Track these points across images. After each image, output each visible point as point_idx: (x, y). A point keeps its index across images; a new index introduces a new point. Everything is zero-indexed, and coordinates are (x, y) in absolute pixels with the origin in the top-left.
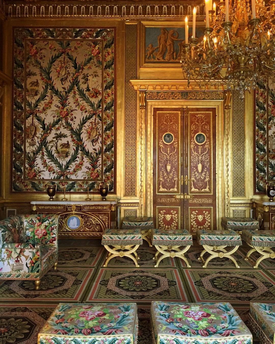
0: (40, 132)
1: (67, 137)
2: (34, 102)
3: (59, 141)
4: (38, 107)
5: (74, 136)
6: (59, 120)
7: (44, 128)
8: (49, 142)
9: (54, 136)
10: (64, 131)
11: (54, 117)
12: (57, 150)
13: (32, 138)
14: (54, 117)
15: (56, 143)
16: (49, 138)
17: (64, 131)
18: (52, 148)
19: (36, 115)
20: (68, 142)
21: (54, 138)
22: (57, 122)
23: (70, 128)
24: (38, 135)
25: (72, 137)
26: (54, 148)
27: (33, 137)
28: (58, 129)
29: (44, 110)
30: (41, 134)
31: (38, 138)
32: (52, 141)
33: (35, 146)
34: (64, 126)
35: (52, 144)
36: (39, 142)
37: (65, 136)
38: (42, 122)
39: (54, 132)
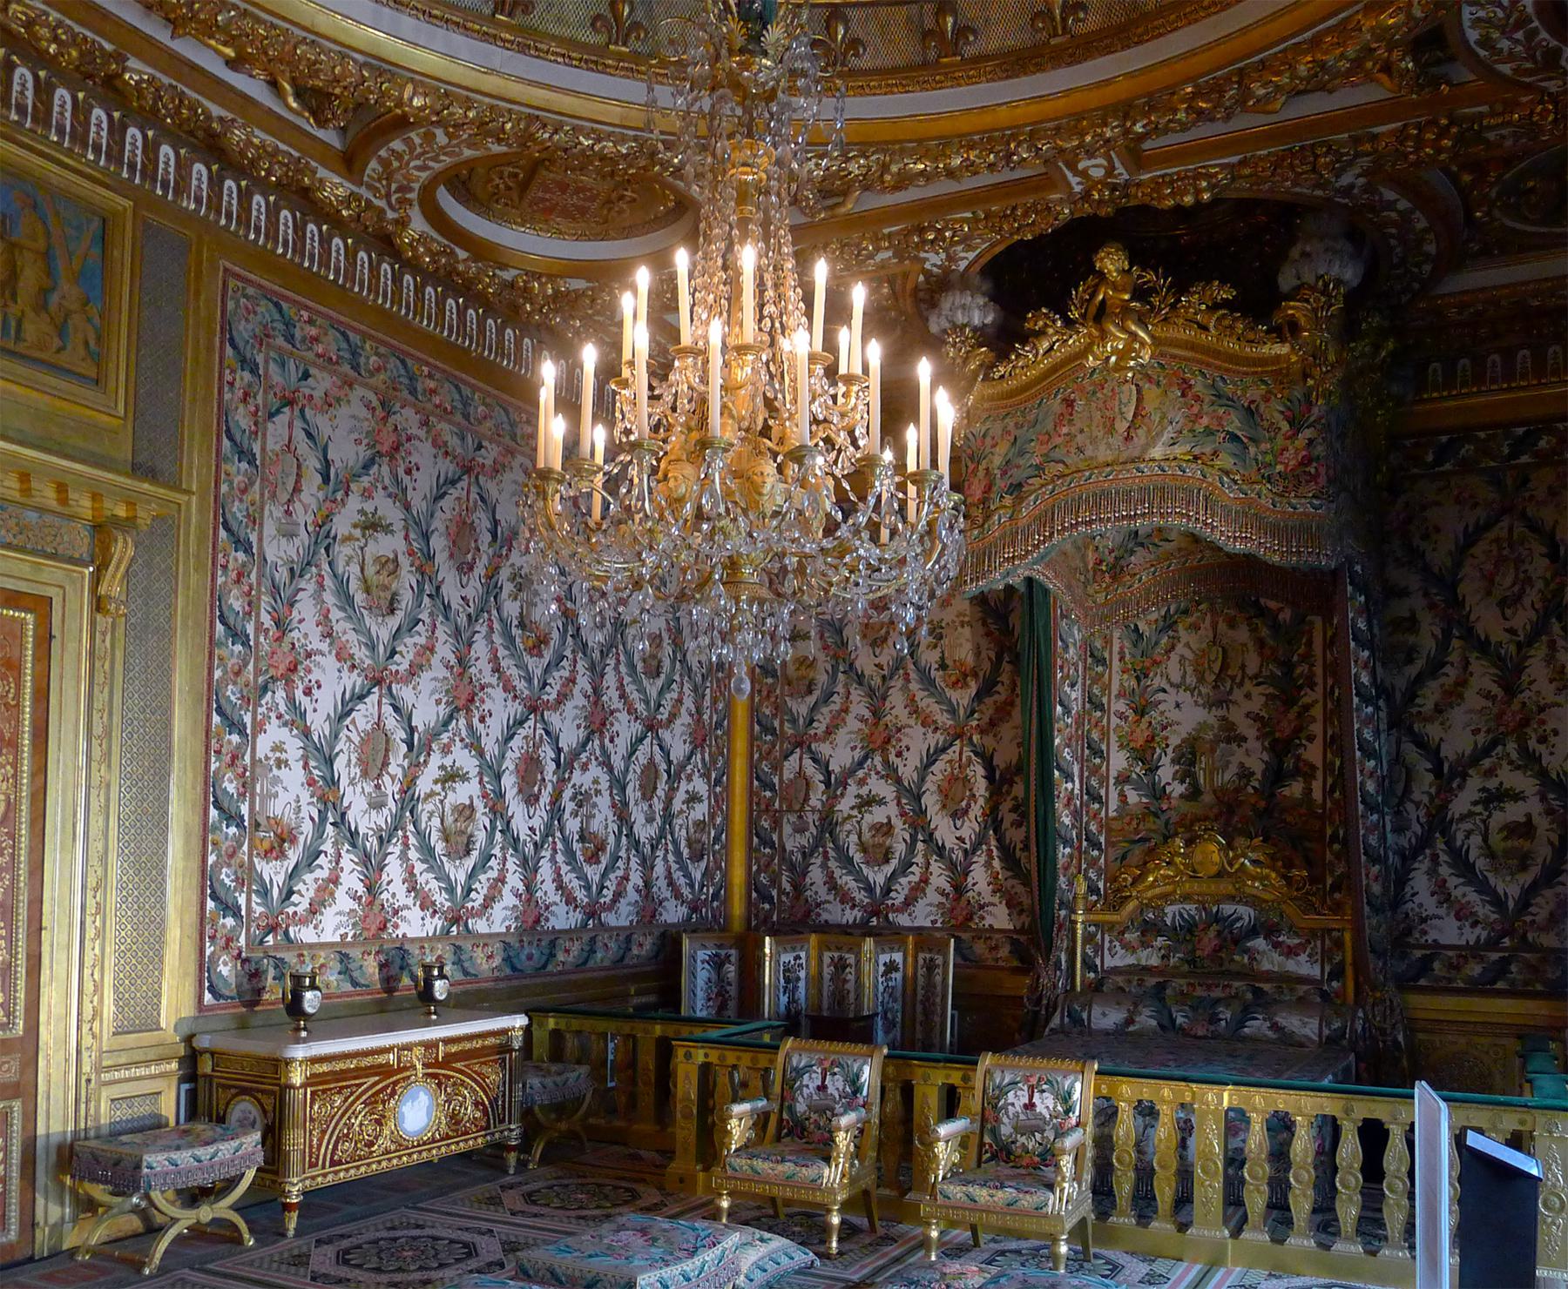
0: (1424, 784)
1: (1524, 799)
2: (1401, 683)
3: (1497, 815)
4: (1418, 701)
5: (1551, 796)
6: (1494, 743)
7: (1437, 771)
8: (1457, 816)
9: (1476, 796)
10: (1510, 778)
11: (1476, 732)
12: (1489, 847)
13: (1398, 805)
14: (1476, 732)
15: (1484, 821)
16: (1461, 803)
17: (1510, 778)
18: (1467, 837)
19: (1410, 730)
20: (1529, 816)
21: (1475, 803)
22: (1486, 751)
23: (1537, 768)
24: (1416, 796)
25: (1543, 799)
26: (1476, 840)
27: (1401, 803)
28: (1490, 773)
29: (1439, 710)
30: (1429, 794)
31: (1417, 805)
32: (1471, 814)
34: (1511, 763)
35: (1467, 826)
36: (1423, 820)
37: (1517, 797)
38: (1433, 753)
39: (1474, 784)
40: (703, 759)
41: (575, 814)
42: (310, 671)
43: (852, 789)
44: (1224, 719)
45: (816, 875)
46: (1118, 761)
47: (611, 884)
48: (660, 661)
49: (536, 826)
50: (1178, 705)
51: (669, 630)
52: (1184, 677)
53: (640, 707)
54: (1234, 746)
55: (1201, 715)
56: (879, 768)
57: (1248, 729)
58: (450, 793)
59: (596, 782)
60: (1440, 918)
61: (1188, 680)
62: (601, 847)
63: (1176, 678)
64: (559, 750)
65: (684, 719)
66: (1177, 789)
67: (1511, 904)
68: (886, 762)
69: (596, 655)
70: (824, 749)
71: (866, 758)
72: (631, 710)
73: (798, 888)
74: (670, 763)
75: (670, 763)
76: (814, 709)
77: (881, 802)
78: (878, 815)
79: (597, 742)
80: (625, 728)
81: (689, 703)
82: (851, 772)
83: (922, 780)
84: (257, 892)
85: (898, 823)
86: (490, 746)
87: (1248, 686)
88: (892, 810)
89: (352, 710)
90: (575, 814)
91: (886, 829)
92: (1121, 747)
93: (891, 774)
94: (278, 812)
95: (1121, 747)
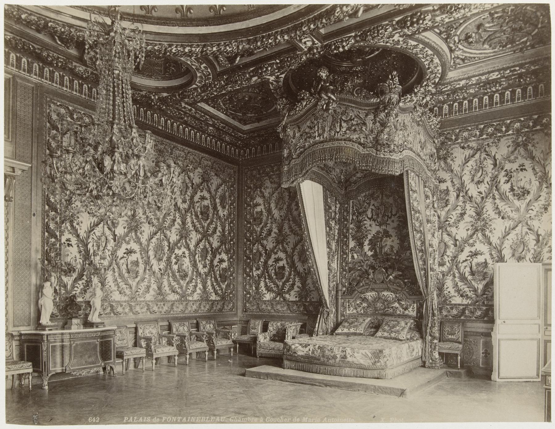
0: (451, 251)
3: (475, 259)
7: (455, 245)
8: (461, 261)
13: (442, 256)
15: (471, 262)
16: (462, 257)
20: (486, 260)
24: (448, 253)
28: (472, 245)
31: (448, 256)
32: (466, 260)
33: (446, 266)
40: (225, 247)
41: (176, 263)
42: (78, 218)
43: (273, 256)
44: (385, 230)
45: (262, 284)
46: (352, 244)
47: (191, 288)
48: (208, 215)
49: (162, 268)
50: (370, 225)
51: (212, 204)
52: (373, 215)
53: (201, 230)
54: (388, 239)
55: (378, 228)
56: (281, 248)
57: (392, 232)
58: (130, 257)
59: (184, 253)
60: (455, 296)
61: (374, 217)
62: (186, 275)
63: (370, 216)
64: (169, 243)
65: (218, 233)
66: (370, 253)
67: (479, 291)
68: (283, 246)
69: (183, 212)
70: (265, 242)
71: (277, 246)
72: (197, 231)
73: (257, 288)
74: (212, 248)
75: (212, 248)
76: (262, 229)
77: (282, 260)
78: (281, 264)
79: (184, 241)
80: (194, 237)
81: (219, 228)
82: (272, 251)
83: (294, 252)
84: (63, 286)
85: (286, 266)
86: (144, 241)
87: (393, 218)
88: (284, 262)
89: (94, 229)
90: (176, 263)
91: (283, 268)
92: (353, 240)
93: (285, 251)
94: (69, 260)
95: (353, 240)
